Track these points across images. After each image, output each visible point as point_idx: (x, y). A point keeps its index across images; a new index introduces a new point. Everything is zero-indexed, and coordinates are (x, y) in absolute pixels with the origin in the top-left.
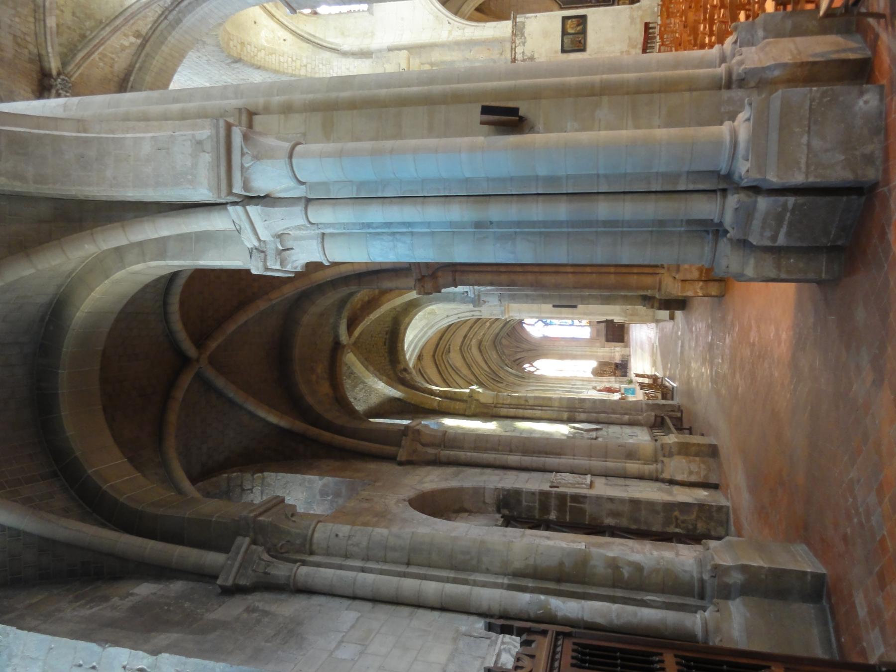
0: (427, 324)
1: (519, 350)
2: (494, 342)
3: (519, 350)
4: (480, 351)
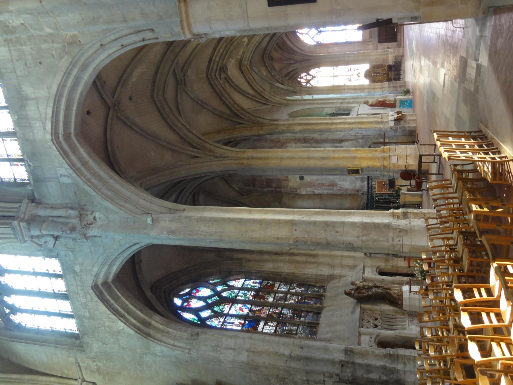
0: (72, 65)
1: (292, 62)
2: (263, 57)
3: (292, 62)
4: (242, 73)
